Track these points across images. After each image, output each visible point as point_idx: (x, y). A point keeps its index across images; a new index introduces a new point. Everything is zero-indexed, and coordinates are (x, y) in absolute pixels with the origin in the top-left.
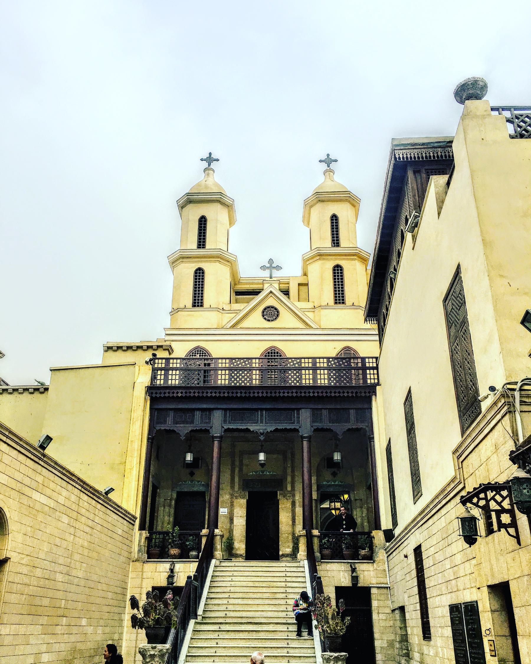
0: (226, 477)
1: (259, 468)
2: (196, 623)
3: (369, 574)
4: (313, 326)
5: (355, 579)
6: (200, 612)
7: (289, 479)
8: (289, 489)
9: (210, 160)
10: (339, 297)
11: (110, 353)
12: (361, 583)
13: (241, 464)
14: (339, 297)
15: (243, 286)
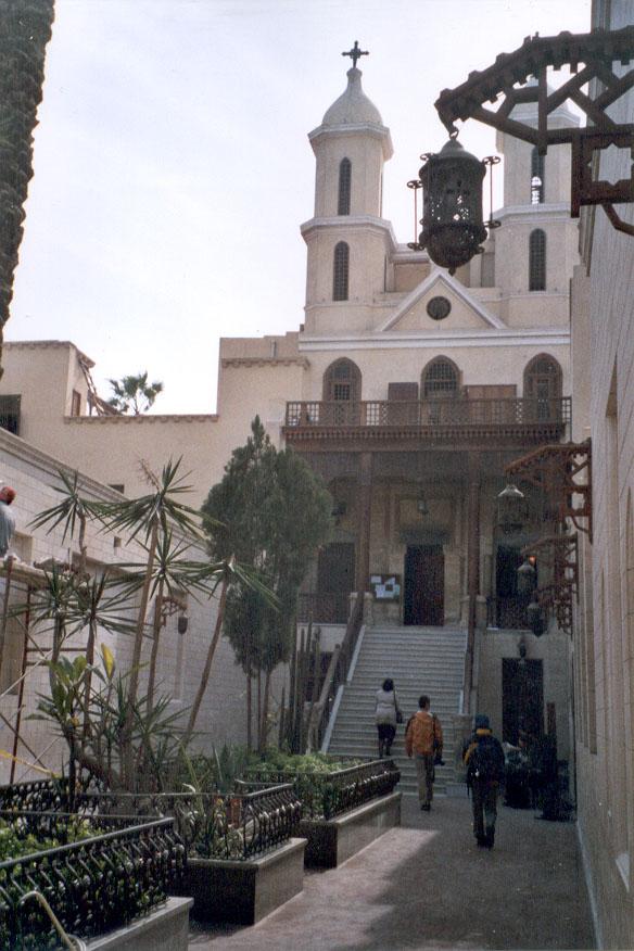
0: (377, 526)
1: (421, 516)
2: (345, 689)
3: (540, 646)
4: (497, 326)
5: (523, 652)
6: (349, 678)
7: (458, 530)
8: (457, 542)
9: (356, 54)
10: (537, 282)
11: (231, 370)
12: (532, 655)
13: (398, 511)
14: (537, 282)
15: (402, 255)
